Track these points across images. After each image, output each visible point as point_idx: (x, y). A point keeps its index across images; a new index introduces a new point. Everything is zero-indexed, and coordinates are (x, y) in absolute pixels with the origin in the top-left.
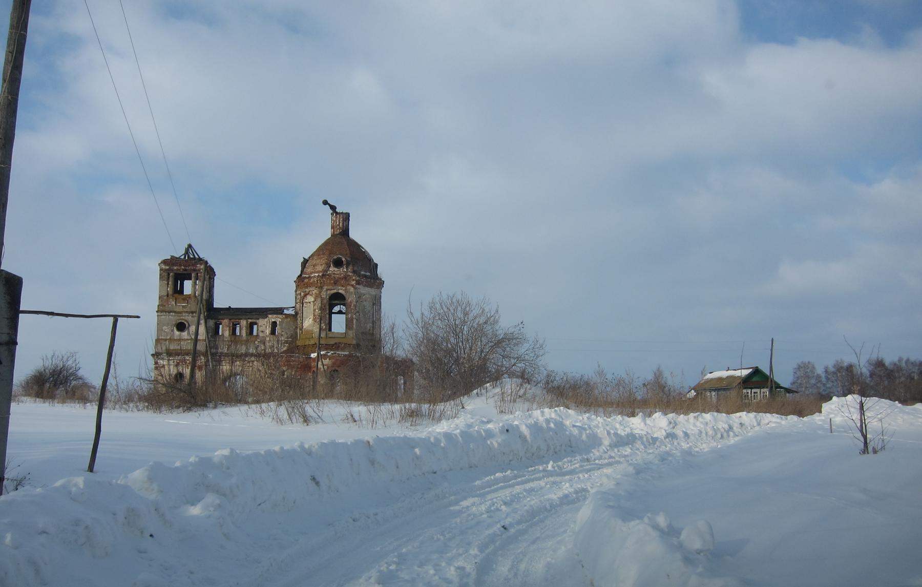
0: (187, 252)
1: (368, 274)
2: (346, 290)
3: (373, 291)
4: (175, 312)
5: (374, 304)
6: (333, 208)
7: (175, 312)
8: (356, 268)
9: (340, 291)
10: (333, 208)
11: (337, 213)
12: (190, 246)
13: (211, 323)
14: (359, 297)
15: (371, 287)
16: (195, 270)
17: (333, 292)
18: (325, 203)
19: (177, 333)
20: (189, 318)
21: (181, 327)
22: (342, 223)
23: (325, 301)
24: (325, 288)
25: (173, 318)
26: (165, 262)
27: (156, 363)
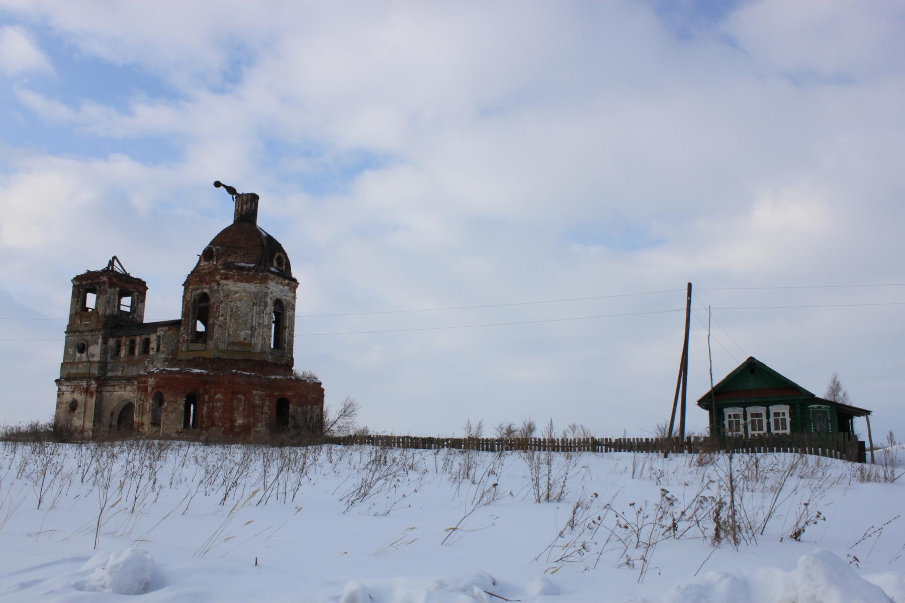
0: (111, 263)
1: (251, 265)
2: (211, 288)
3: (275, 289)
4: (78, 331)
5: (254, 304)
6: (231, 190)
7: (78, 331)
8: (231, 259)
9: (206, 290)
10: (231, 190)
11: (238, 195)
12: (115, 258)
13: (112, 342)
14: (227, 296)
15: (247, 282)
16: (99, 283)
17: (200, 291)
18: (218, 184)
19: (78, 355)
20: (88, 337)
21: (82, 349)
22: (247, 207)
23: (190, 305)
24: (191, 287)
25: (76, 338)
26: (78, 279)
27: (59, 389)
